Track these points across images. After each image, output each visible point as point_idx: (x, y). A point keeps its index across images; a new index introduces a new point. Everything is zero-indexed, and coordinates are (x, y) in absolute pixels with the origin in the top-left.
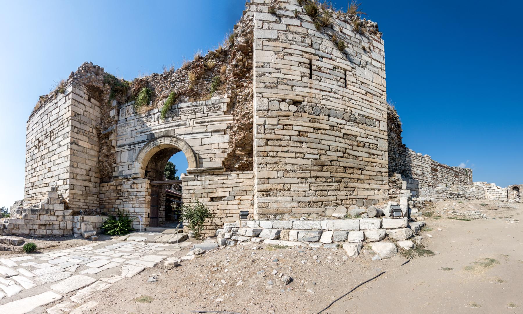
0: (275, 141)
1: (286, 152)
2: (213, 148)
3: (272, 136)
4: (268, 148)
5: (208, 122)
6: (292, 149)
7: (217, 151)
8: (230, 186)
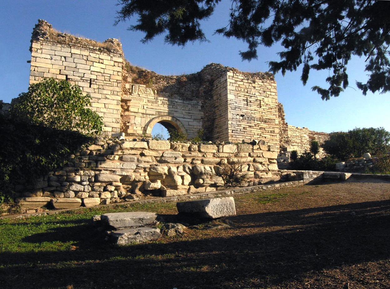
3: (234, 129)
4: (233, 134)
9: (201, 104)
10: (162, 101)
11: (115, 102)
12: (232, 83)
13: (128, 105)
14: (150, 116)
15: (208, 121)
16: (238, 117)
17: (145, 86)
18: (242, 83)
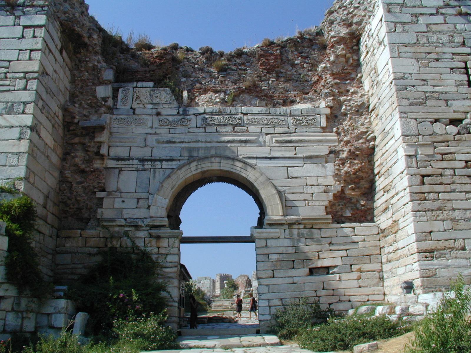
0: (434, 177)
1: (451, 192)
2: (308, 183)
3: (429, 171)
4: (426, 188)
5: (297, 141)
6: (459, 188)
7: (315, 189)
8: (342, 247)
9: (328, 111)
10: (199, 117)
11: (16, 133)
12: (403, 24)
13: (97, 139)
14: (164, 163)
15: (353, 155)
16: (438, 128)
17: (151, 84)
18: (439, 19)
